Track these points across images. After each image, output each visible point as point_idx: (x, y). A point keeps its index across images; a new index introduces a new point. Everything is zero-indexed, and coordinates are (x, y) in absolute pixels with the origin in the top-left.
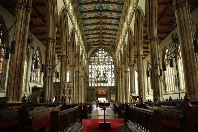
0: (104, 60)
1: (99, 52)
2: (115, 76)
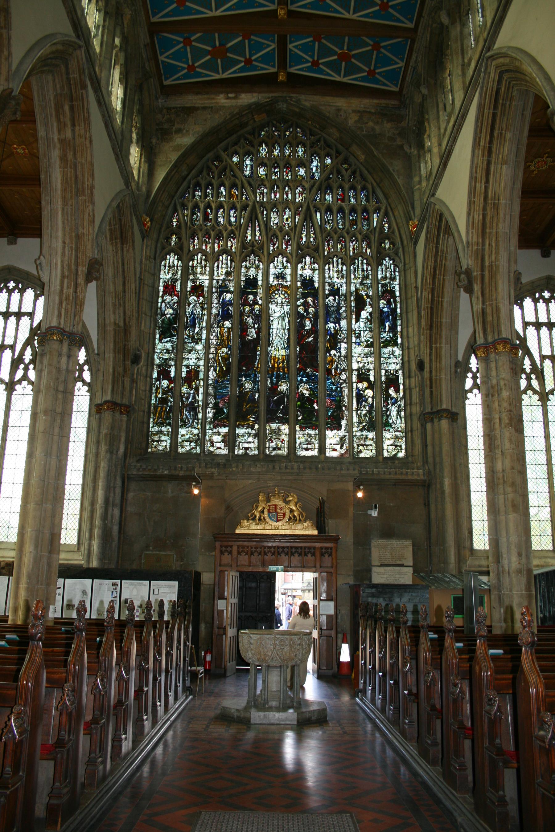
0: (308, 218)
1: (263, 151)
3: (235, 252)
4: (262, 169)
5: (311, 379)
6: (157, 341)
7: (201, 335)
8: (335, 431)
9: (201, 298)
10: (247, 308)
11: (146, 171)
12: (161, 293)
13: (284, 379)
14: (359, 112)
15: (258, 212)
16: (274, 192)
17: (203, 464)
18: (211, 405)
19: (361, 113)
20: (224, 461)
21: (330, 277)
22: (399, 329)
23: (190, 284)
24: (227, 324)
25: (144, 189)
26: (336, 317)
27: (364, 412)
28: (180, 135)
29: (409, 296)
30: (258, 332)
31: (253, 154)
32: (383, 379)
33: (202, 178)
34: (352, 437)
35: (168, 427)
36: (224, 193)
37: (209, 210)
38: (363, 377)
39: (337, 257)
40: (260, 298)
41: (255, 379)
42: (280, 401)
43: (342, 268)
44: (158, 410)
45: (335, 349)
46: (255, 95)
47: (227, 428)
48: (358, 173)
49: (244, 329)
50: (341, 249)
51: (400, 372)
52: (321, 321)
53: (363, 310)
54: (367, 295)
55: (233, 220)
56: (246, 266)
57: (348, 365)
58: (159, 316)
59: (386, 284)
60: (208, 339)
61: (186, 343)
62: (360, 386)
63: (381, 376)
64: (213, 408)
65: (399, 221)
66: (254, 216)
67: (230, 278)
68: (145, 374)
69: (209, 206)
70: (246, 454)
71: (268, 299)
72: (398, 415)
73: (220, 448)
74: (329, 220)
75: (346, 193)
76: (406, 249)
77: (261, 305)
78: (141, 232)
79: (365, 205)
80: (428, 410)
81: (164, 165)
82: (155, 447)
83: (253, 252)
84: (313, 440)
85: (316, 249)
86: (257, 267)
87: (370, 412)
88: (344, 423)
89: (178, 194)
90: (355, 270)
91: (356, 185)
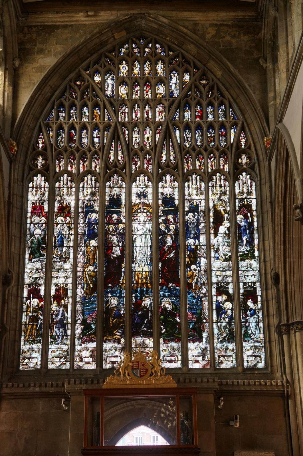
0: (168, 136)
1: (124, 69)
2: (263, 274)
3: (99, 174)
4: (123, 89)
5: (173, 294)
6: (27, 261)
7: (69, 254)
8: (196, 344)
9: (68, 218)
10: (112, 227)
11: (11, 94)
12: (29, 215)
13: (147, 293)
14: (216, 25)
15: (120, 132)
16: (135, 112)
17: (72, 381)
18: (79, 322)
19: (218, 26)
20: (92, 376)
21: (189, 194)
22: (256, 242)
23: (57, 205)
24: (93, 243)
25: (9, 113)
26: (196, 233)
27: (224, 324)
28: (42, 56)
29: (265, 210)
30: (122, 251)
31: (114, 71)
32: (242, 291)
33: (65, 100)
34: (213, 348)
35: (39, 344)
36: (87, 114)
37: (73, 131)
38: (222, 290)
39: (196, 174)
40: (124, 217)
41: (120, 295)
42: (145, 315)
43: (200, 185)
44: (29, 327)
45: (195, 265)
46: (114, 12)
47: (95, 343)
48: (215, 88)
49: (109, 247)
50: (200, 166)
51: (258, 284)
52: (181, 238)
53: (221, 225)
54: (224, 210)
55: (96, 140)
56: (110, 186)
57: (207, 279)
58: (28, 237)
59: (243, 199)
60: (75, 258)
61: (54, 262)
62: (220, 298)
63: (239, 289)
64: (81, 324)
65: (255, 137)
66: (116, 137)
67: (95, 198)
68: (16, 293)
69: (72, 127)
70: (113, 368)
71: (131, 217)
72: (257, 326)
73: (88, 363)
74: (188, 138)
75: (204, 111)
76: (262, 164)
77: (124, 223)
78: (9, 157)
79: (222, 122)
80: (284, 322)
81: (28, 87)
82: (26, 364)
83: (116, 172)
84: (176, 352)
85: (176, 167)
86: (120, 187)
87: (229, 323)
88: (205, 335)
89: (42, 116)
90: (213, 186)
91: (213, 101)
